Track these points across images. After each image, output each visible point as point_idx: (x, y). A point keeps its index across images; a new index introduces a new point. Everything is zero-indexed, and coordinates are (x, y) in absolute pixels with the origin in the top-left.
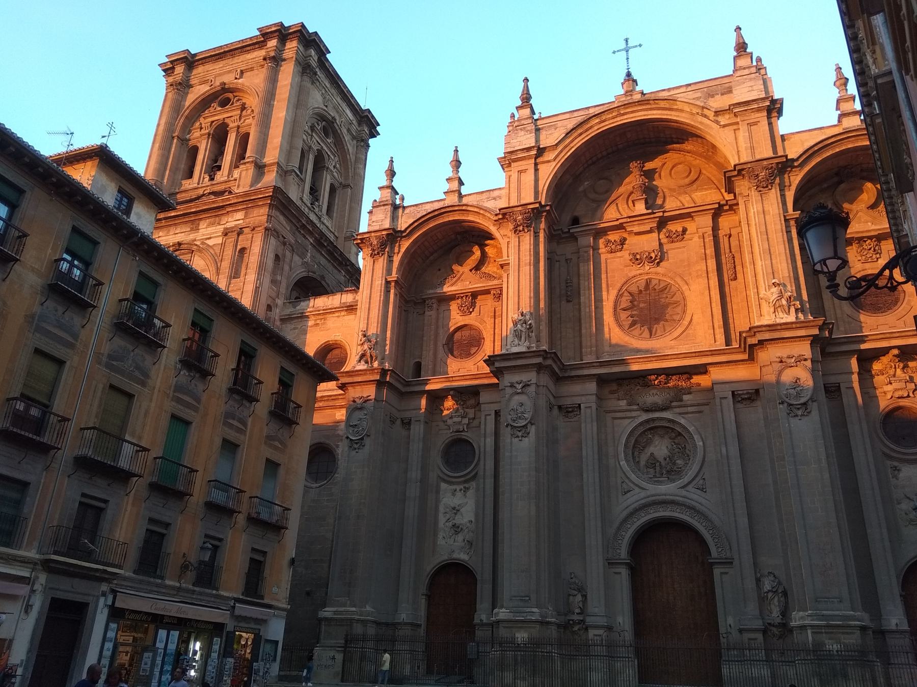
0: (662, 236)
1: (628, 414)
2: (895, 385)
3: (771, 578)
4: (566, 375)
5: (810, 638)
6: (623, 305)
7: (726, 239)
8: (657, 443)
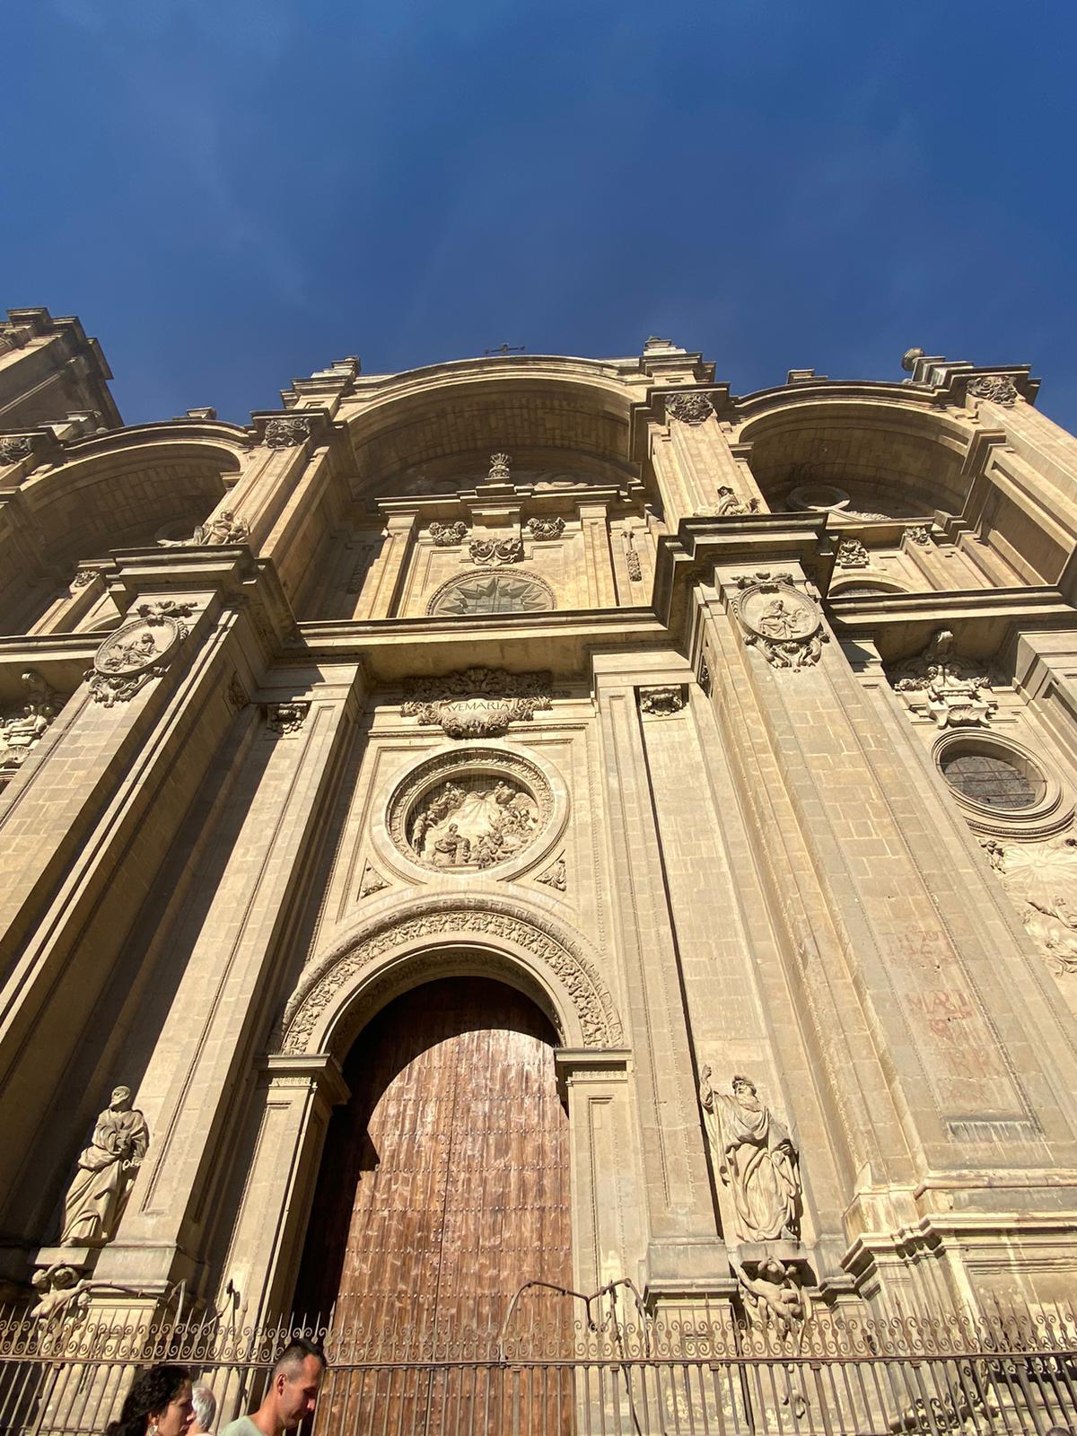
0: (528, 529)
1: (417, 742)
2: (951, 701)
3: (745, 1097)
4: (296, 646)
5: (966, 1294)
6: (447, 605)
7: (625, 540)
8: (468, 809)
